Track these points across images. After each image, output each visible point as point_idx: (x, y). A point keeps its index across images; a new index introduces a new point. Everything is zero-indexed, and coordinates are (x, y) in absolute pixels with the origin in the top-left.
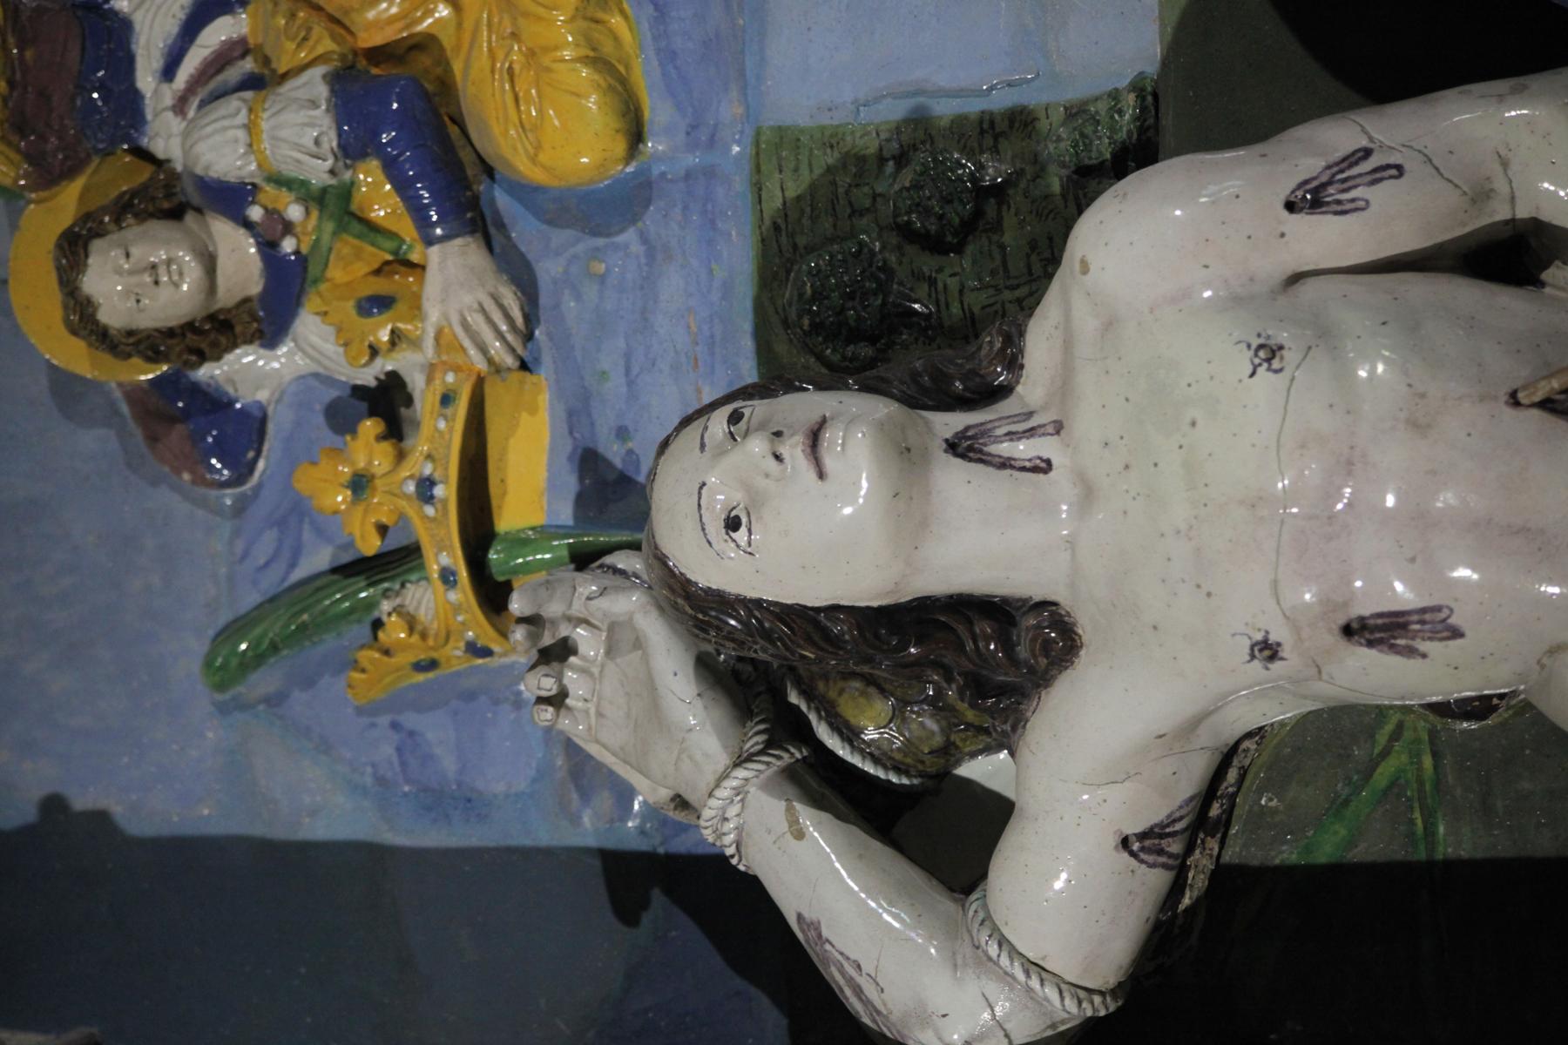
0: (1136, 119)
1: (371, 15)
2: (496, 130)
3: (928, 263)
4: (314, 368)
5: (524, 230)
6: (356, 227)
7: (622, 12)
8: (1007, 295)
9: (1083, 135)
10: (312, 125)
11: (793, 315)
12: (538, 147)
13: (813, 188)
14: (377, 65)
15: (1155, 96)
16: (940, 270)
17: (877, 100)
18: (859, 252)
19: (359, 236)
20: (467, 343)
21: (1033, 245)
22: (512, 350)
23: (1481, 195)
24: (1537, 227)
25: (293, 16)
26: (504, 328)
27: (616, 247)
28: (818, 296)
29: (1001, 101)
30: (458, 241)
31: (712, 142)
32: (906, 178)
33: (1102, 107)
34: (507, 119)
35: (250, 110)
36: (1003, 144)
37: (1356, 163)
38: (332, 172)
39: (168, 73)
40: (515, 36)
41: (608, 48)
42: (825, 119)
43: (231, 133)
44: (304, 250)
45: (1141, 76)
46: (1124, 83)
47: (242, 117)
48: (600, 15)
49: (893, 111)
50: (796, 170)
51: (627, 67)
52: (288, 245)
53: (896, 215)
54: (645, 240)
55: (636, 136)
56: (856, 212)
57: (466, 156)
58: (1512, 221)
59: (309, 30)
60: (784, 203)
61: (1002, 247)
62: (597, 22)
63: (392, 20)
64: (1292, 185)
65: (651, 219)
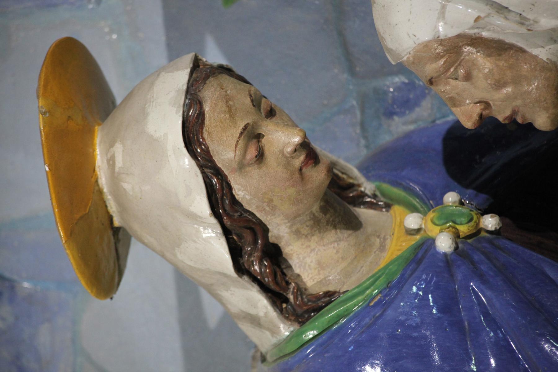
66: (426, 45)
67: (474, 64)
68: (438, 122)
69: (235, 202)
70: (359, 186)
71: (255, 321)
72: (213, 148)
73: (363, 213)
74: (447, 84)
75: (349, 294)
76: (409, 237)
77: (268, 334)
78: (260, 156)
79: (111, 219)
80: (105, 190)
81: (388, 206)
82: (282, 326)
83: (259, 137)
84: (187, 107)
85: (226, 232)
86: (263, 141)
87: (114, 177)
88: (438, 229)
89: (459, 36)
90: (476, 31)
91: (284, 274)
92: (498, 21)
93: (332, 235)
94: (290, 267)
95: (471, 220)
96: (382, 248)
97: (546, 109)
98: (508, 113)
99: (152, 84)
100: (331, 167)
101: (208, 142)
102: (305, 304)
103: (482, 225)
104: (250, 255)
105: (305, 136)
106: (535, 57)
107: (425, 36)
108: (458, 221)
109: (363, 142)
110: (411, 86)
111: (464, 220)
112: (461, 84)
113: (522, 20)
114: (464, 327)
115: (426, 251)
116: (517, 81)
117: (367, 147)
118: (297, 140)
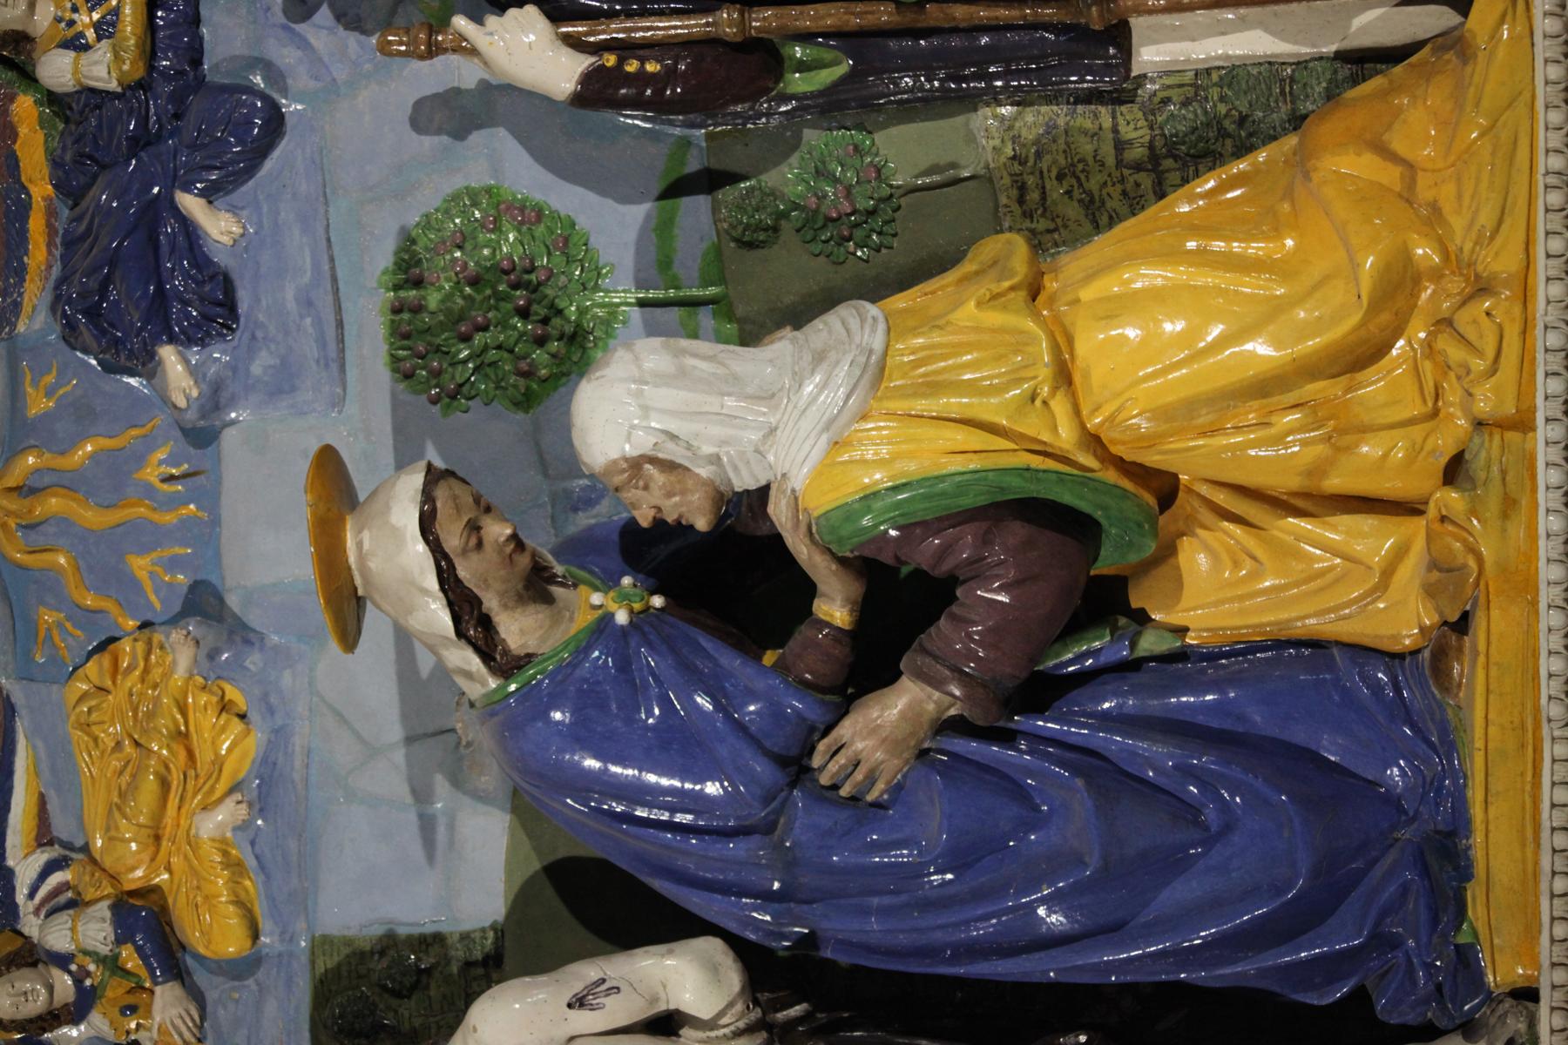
0: (492, 943)
1: (131, 876)
2: (189, 931)
3: (394, 1002)
4: (96, 1034)
5: (201, 978)
6: (120, 972)
7: (250, 878)
8: (431, 1019)
9: (469, 949)
10: (103, 931)
11: (329, 1022)
12: (209, 942)
13: (339, 965)
14: (132, 897)
15: (502, 931)
16: (400, 1006)
17: (371, 925)
18: (361, 996)
19: (121, 977)
20: (174, 1033)
21: (444, 997)
22: (194, 1035)
23: (654, 1000)
24: (677, 1012)
25: (93, 875)
26: (191, 1025)
27: (244, 986)
28: (341, 1016)
29: (429, 929)
30: (170, 984)
31: (291, 939)
32: (385, 963)
33: (477, 935)
34: (194, 927)
35: (73, 921)
36: (430, 949)
37: (598, 986)
38: (111, 951)
39: (31, 895)
40: (198, 888)
41: (243, 895)
42: (346, 933)
43: (64, 932)
44: (95, 984)
45: (495, 922)
46: (487, 924)
47: (69, 924)
48: (240, 880)
49: (378, 930)
50: (332, 955)
51: (252, 905)
52: (88, 982)
53: (380, 980)
54: (258, 984)
55: (255, 935)
56: (360, 977)
57: (173, 941)
58: (668, 1010)
59: (101, 883)
60: (326, 970)
61: (430, 998)
62: (238, 883)
63: (140, 878)
64: (571, 996)
65: (260, 974)
66: (615, 462)
67: (651, 477)
68: (615, 518)
69: (458, 581)
70: (552, 568)
71: (468, 675)
72: (442, 536)
73: (557, 591)
74: (629, 491)
75: (545, 656)
76: (593, 612)
77: (478, 686)
78: (480, 545)
79: (356, 589)
80: (353, 567)
81: (575, 586)
82: (490, 680)
83: (478, 529)
84: (423, 503)
85: (450, 604)
86: (482, 532)
87: (361, 557)
88: (616, 606)
89: (641, 456)
90: (654, 453)
91: (493, 639)
92: (671, 445)
93: (532, 608)
94: (497, 633)
95: (642, 600)
96: (571, 619)
97: (705, 515)
98: (675, 516)
99: (394, 484)
100: (534, 555)
101: (439, 532)
102: (508, 663)
103: (651, 604)
104: (468, 622)
105: (515, 529)
106: (698, 475)
107: (614, 455)
108: (633, 599)
109: (552, 531)
110: (592, 488)
111: (638, 599)
112: (640, 493)
113: (689, 447)
114: (636, 684)
115: (607, 624)
116: (683, 493)
117: (556, 536)
118: (509, 531)
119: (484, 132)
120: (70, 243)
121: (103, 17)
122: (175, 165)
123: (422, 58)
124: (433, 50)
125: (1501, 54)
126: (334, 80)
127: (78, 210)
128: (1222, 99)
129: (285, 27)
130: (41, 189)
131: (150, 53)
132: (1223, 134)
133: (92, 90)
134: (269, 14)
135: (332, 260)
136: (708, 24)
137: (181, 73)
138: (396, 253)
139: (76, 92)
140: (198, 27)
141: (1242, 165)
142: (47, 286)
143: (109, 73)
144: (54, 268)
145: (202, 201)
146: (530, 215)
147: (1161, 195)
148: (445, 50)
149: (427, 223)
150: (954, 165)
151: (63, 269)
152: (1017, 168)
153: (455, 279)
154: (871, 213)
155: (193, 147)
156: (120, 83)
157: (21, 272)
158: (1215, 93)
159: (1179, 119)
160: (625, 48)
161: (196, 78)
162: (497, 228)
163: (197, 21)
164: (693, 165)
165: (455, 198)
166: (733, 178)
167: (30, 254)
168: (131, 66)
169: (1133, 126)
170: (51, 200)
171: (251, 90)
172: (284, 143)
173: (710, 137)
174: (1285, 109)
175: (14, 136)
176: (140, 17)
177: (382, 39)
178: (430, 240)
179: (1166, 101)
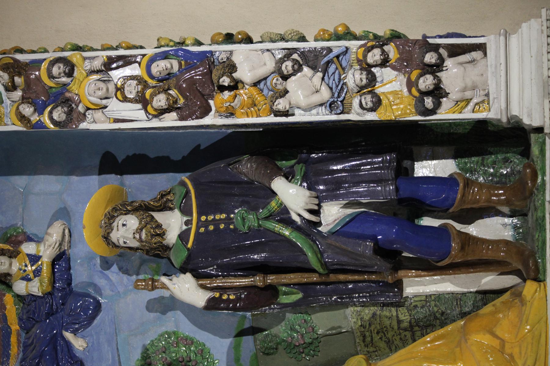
119: (173, 312)
120: (26, 347)
121: (36, 268)
122: (62, 322)
123: (150, 291)
124: (154, 288)
125: (536, 303)
126: (119, 292)
127: (28, 335)
128: (435, 306)
129: (101, 272)
130: (15, 327)
131: (53, 281)
132: (436, 318)
133: (33, 295)
134: (95, 267)
135: (119, 355)
136: (252, 281)
137: (64, 289)
138: (142, 354)
139: (27, 295)
140: (70, 271)
141: (441, 331)
142: (18, 361)
143: (39, 290)
144: (20, 355)
145: (72, 335)
146: (189, 341)
147: (414, 341)
148: (158, 288)
149: (152, 343)
150: (340, 327)
151: (23, 356)
152: (362, 329)
153: (163, 363)
154: (311, 344)
155: (69, 315)
156: (42, 293)
157: (8, 356)
158: (433, 303)
159: (421, 313)
160: (222, 289)
161: (69, 290)
162: (177, 346)
163: (70, 268)
164: (247, 325)
165: (162, 335)
166: (261, 330)
167: (11, 350)
168: (47, 288)
169: (404, 315)
170: (19, 330)
171: (89, 295)
172: (101, 314)
173: (253, 315)
174: (458, 310)
175: (5, 309)
176: (49, 270)
177: (136, 284)
178: (153, 349)
179: (416, 306)
